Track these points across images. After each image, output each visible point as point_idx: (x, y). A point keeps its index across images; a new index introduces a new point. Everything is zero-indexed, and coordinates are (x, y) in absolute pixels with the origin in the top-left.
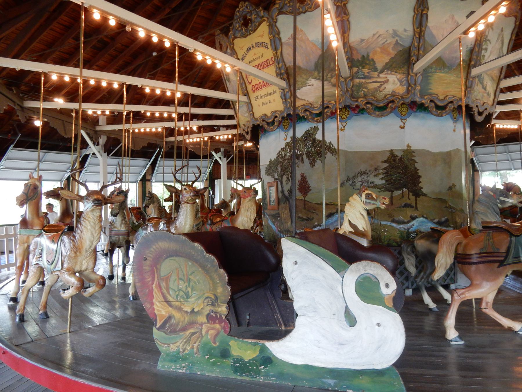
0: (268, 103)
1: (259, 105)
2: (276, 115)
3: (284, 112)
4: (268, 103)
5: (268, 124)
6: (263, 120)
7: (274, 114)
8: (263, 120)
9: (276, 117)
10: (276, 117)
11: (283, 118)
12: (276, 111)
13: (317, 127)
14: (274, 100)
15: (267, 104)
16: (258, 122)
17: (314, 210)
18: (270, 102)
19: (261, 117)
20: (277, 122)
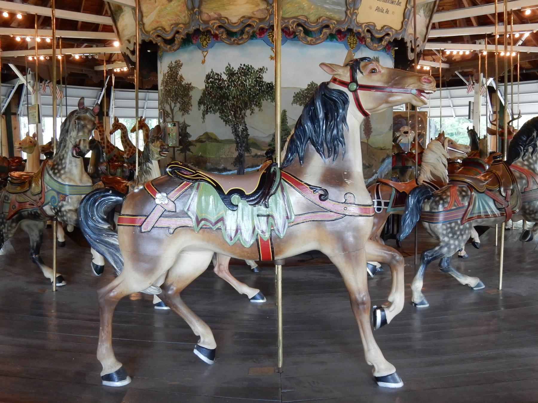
0: (385, 11)
1: (371, 8)
2: (390, 32)
3: (399, 34)
4: (385, 11)
5: (373, 38)
6: (368, 31)
7: (387, 30)
8: (368, 31)
9: (388, 34)
10: (388, 34)
11: (395, 40)
12: (391, 28)
13: (378, 59)
14: (393, 13)
15: (382, 12)
16: (360, 30)
17: (374, 155)
18: (387, 12)
19: (368, 24)
20: (386, 40)
